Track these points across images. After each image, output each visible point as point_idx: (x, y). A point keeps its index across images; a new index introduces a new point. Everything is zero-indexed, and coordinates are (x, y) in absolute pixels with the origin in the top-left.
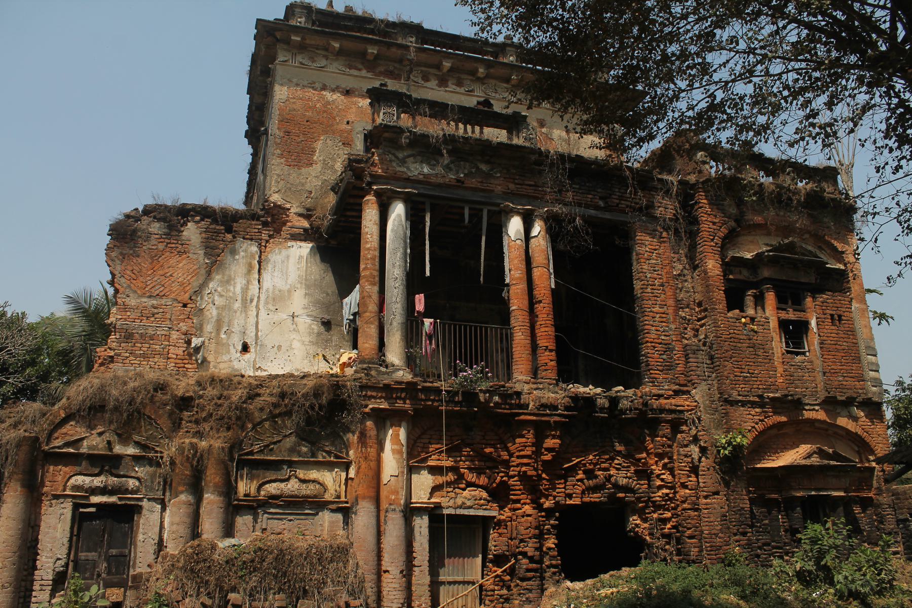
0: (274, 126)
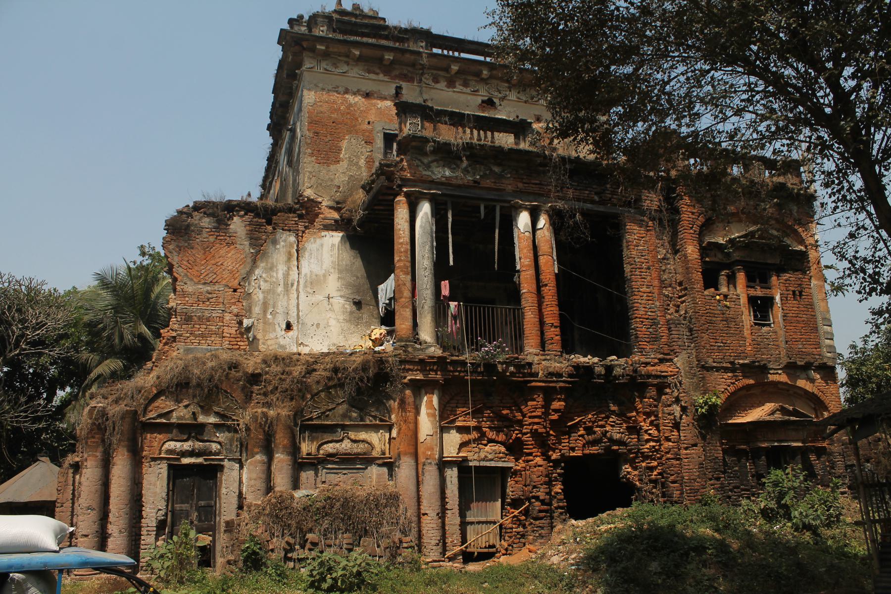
0: (302, 130)
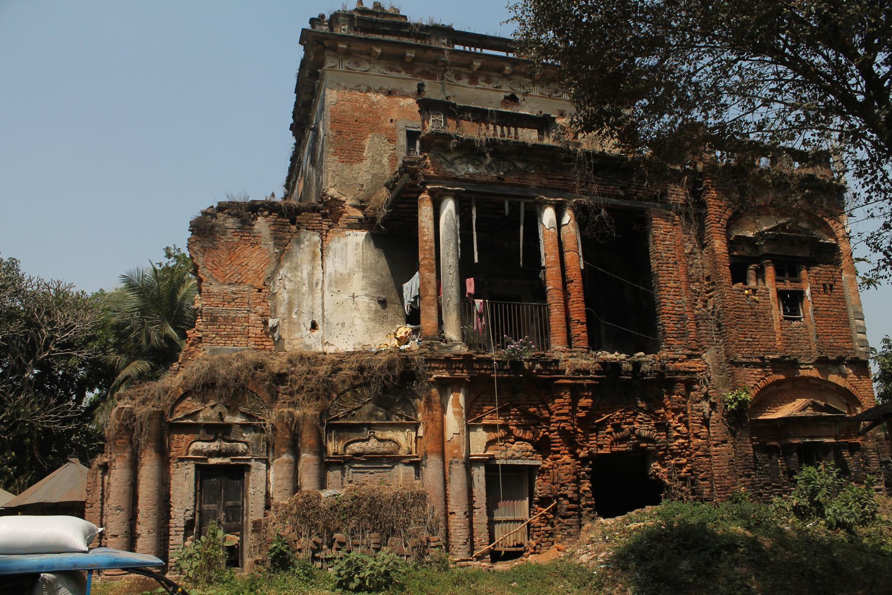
0: (325, 129)
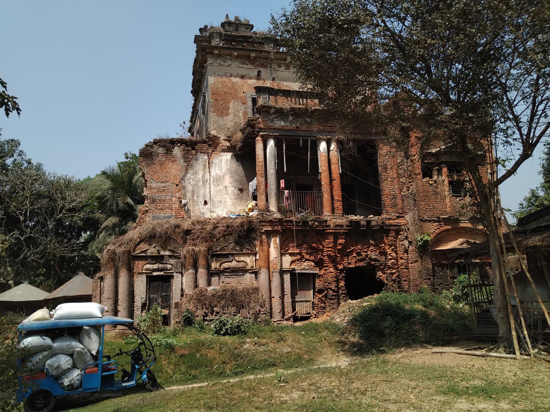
0: (209, 98)
